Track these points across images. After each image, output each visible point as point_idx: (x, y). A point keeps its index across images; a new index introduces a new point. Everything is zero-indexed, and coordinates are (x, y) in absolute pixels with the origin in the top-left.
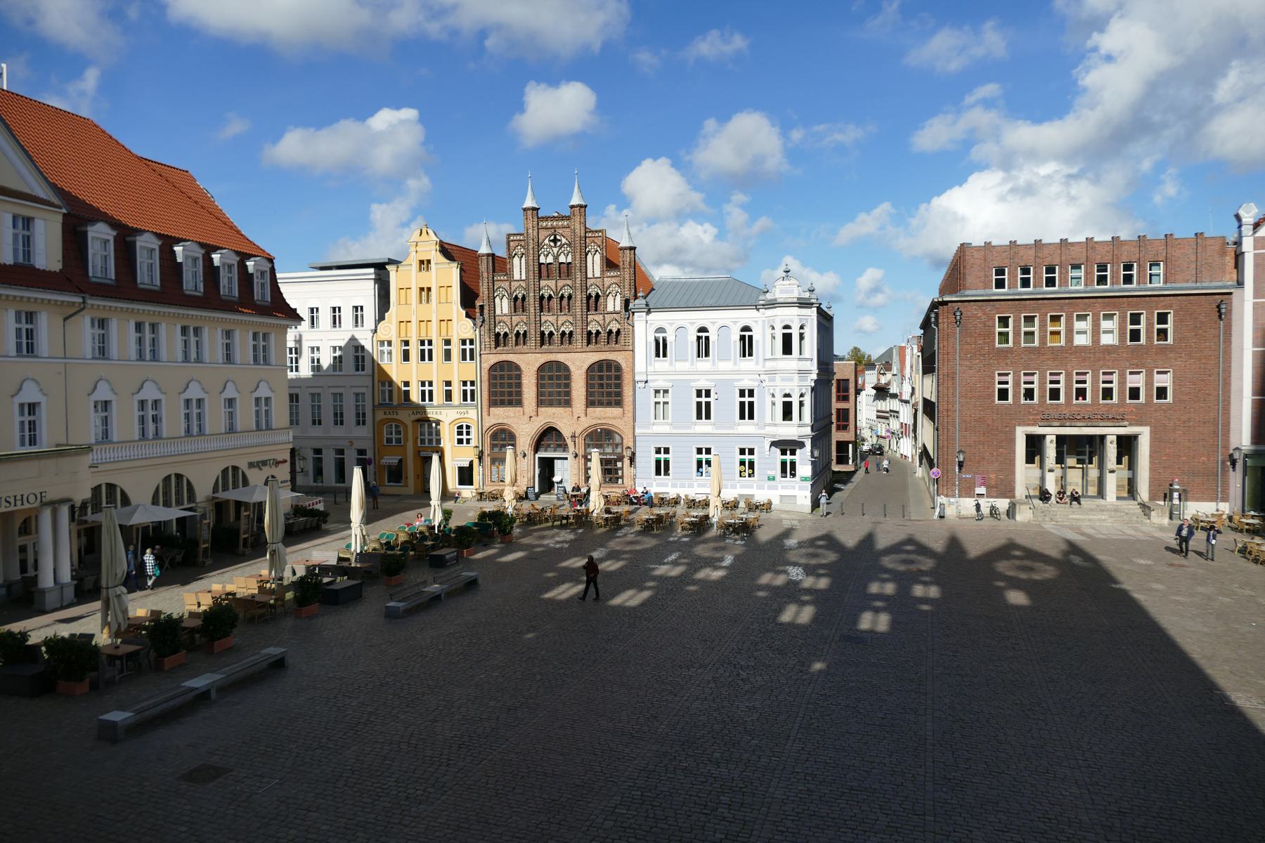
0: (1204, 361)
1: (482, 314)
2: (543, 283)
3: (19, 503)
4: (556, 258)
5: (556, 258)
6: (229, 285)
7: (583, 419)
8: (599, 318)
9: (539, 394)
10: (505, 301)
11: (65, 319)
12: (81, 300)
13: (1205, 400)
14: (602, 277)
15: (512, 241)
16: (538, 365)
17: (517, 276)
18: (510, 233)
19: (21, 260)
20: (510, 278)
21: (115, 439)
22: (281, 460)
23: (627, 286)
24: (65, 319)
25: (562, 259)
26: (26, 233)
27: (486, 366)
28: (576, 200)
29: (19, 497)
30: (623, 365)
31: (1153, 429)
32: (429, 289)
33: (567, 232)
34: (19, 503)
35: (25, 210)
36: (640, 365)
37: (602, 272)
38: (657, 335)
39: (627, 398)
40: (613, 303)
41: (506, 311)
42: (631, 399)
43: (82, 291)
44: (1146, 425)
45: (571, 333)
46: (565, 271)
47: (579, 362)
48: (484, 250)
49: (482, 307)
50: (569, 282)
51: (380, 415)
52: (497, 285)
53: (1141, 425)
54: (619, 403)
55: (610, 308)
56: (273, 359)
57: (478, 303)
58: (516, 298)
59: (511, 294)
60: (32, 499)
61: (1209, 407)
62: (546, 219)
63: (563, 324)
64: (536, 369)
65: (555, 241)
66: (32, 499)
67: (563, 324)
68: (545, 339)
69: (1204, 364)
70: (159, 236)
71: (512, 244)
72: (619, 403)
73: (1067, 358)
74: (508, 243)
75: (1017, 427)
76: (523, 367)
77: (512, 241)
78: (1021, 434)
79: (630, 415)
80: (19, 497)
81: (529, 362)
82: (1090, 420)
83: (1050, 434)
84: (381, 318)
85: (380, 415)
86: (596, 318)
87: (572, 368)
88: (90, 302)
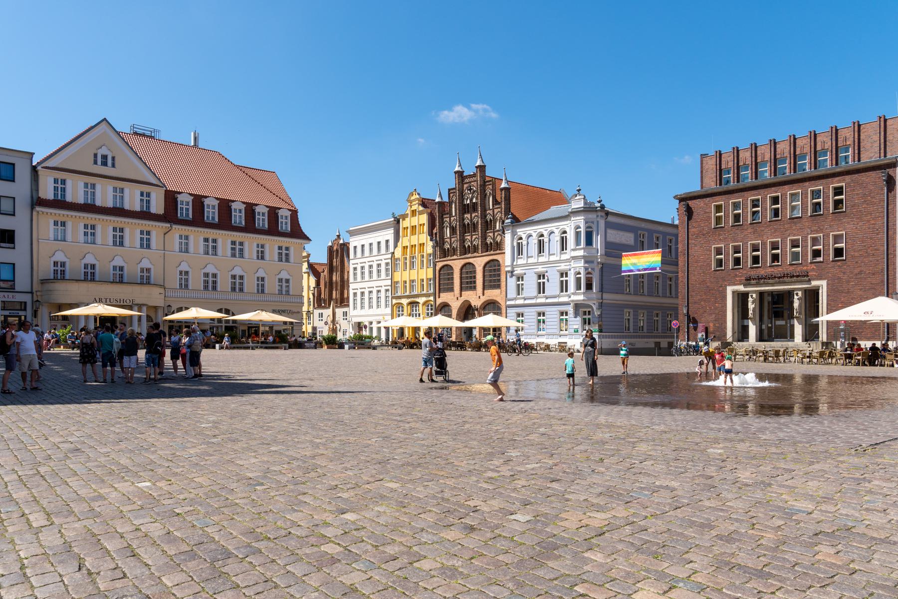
0: (873, 222)
1: (436, 237)
2: (466, 216)
3: (122, 302)
4: (471, 200)
5: (471, 200)
6: (285, 225)
7: (481, 297)
8: (491, 234)
9: (461, 283)
10: (448, 229)
11: (165, 234)
12: (169, 226)
13: (873, 255)
14: (493, 210)
15: (452, 193)
16: (460, 266)
17: (454, 214)
18: (450, 188)
19: (145, 209)
20: (451, 216)
21: (190, 288)
22: (296, 311)
23: (503, 213)
24: (165, 234)
25: (474, 201)
26: (63, 186)
27: (438, 268)
28: (479, 163)
29: (122, 300)
30: (501, 262)
31: (830, 282)
32: (416, 226)
33: (475, 184)
34: (122, 302)
35: (146, 189)
36: (508, 261)
37: (493, 205)
38: (519, 241)
39: (503, 284)
40: (498, 226)
41: (448, 235)
42: (505, 283)
43: (169, 222)
44: (824, 279)
45: (478, 244)
46: (474, 207)
47: (479, 262)
48: (438, 200)
49: (436, 234)
50: (477, 214)
51: (394, 301)
52: (445, 219)
53: (821, 279)
54: (499, 287)
55: (498, 228)
56: (292, 259)
57: (435, 231)
58: (453, 227)
59: (450, 224)
60: (128, 301)
61: (878, 261)
62: (467, 177)
63: (474, 240)
64: (459, 268)
65: (470, 190)
66: (128, 301)
67: (474, 240)
68: (465, 251)
69: (873, 224)
70: (267, 206)
71: (451, 195)
72: (499, 287)
73: (763, 230)
74: (449, 194)
75: (728, 287)
76: (454, 267)
77: (452, 193)
78: (730, 290)
79: (504, 293)
80: (122, 300)
81: (457, 264)
82: (781, 278)
83: (753, 290)
84: (396, 246)
85: (394, 301)
86: (490, 234)
87: (477, 266)
88: (174, 226)
